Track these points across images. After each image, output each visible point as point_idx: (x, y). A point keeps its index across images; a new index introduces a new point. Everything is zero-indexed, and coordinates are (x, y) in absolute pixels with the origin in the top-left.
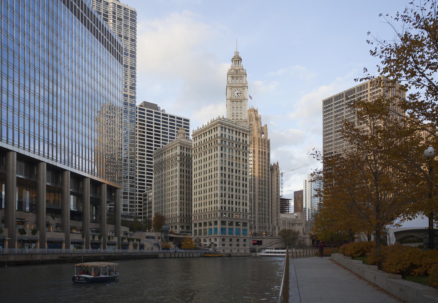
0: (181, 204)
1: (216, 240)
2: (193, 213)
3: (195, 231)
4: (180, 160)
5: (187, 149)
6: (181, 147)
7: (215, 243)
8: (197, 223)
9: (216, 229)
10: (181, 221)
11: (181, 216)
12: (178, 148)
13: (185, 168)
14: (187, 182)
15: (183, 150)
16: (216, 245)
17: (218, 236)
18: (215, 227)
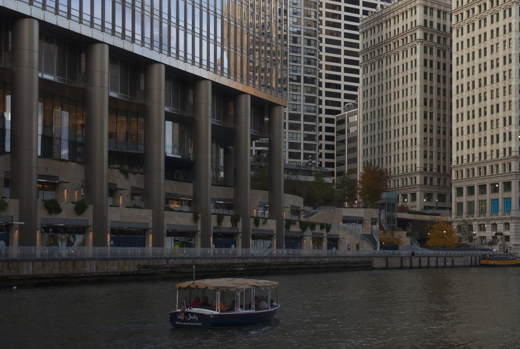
0: (425, 143)
1: (507, 226)
2: (454, 163)
3: (460, 205)
4: (422, 37)
5: (439, 12)
6: (426, 8)
7: (507, 233)
8: (464, 185)
9: (508, 201)
10: (425, 182)
11: (425, 169)
12: (418, 9)
13: (435, 57)
14: (439, 89)
15: (431, 14)
16: (507, 238)
17: (512, 218)
18: (506, 195)
